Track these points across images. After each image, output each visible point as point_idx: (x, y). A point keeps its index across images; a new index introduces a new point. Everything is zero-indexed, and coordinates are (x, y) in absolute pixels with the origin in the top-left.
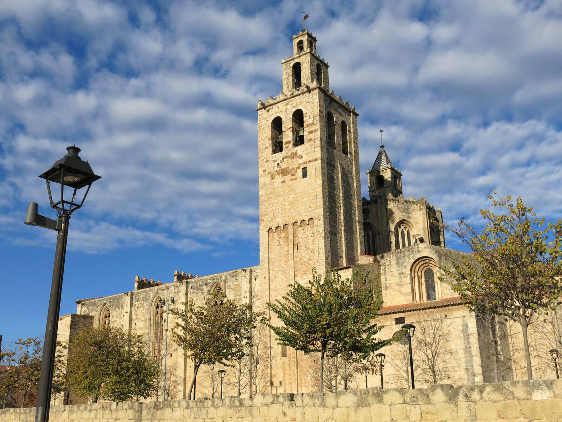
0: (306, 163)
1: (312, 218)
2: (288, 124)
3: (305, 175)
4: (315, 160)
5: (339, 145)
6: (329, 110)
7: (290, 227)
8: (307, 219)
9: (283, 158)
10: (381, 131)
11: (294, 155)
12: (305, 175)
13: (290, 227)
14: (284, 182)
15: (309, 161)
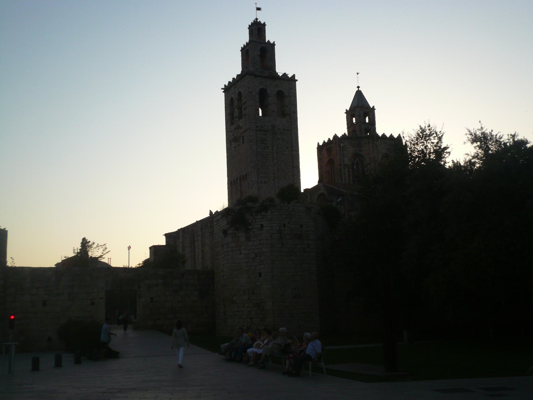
0: (243, 133)
1: (246, 174)
2: (236, 103)
3: (243, 142)
4: (247, 130)
5: (274, 111)
6: (261, 87)
7: (239, 181)
8: (244, 174)
9: (235, 129)
10: (358, 74)
11: (239, 126)
12: (243, 142)
13: (239, 181)
14: (235, 147)
15: (245, 131)
